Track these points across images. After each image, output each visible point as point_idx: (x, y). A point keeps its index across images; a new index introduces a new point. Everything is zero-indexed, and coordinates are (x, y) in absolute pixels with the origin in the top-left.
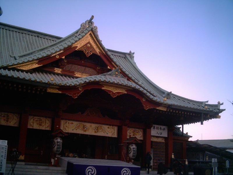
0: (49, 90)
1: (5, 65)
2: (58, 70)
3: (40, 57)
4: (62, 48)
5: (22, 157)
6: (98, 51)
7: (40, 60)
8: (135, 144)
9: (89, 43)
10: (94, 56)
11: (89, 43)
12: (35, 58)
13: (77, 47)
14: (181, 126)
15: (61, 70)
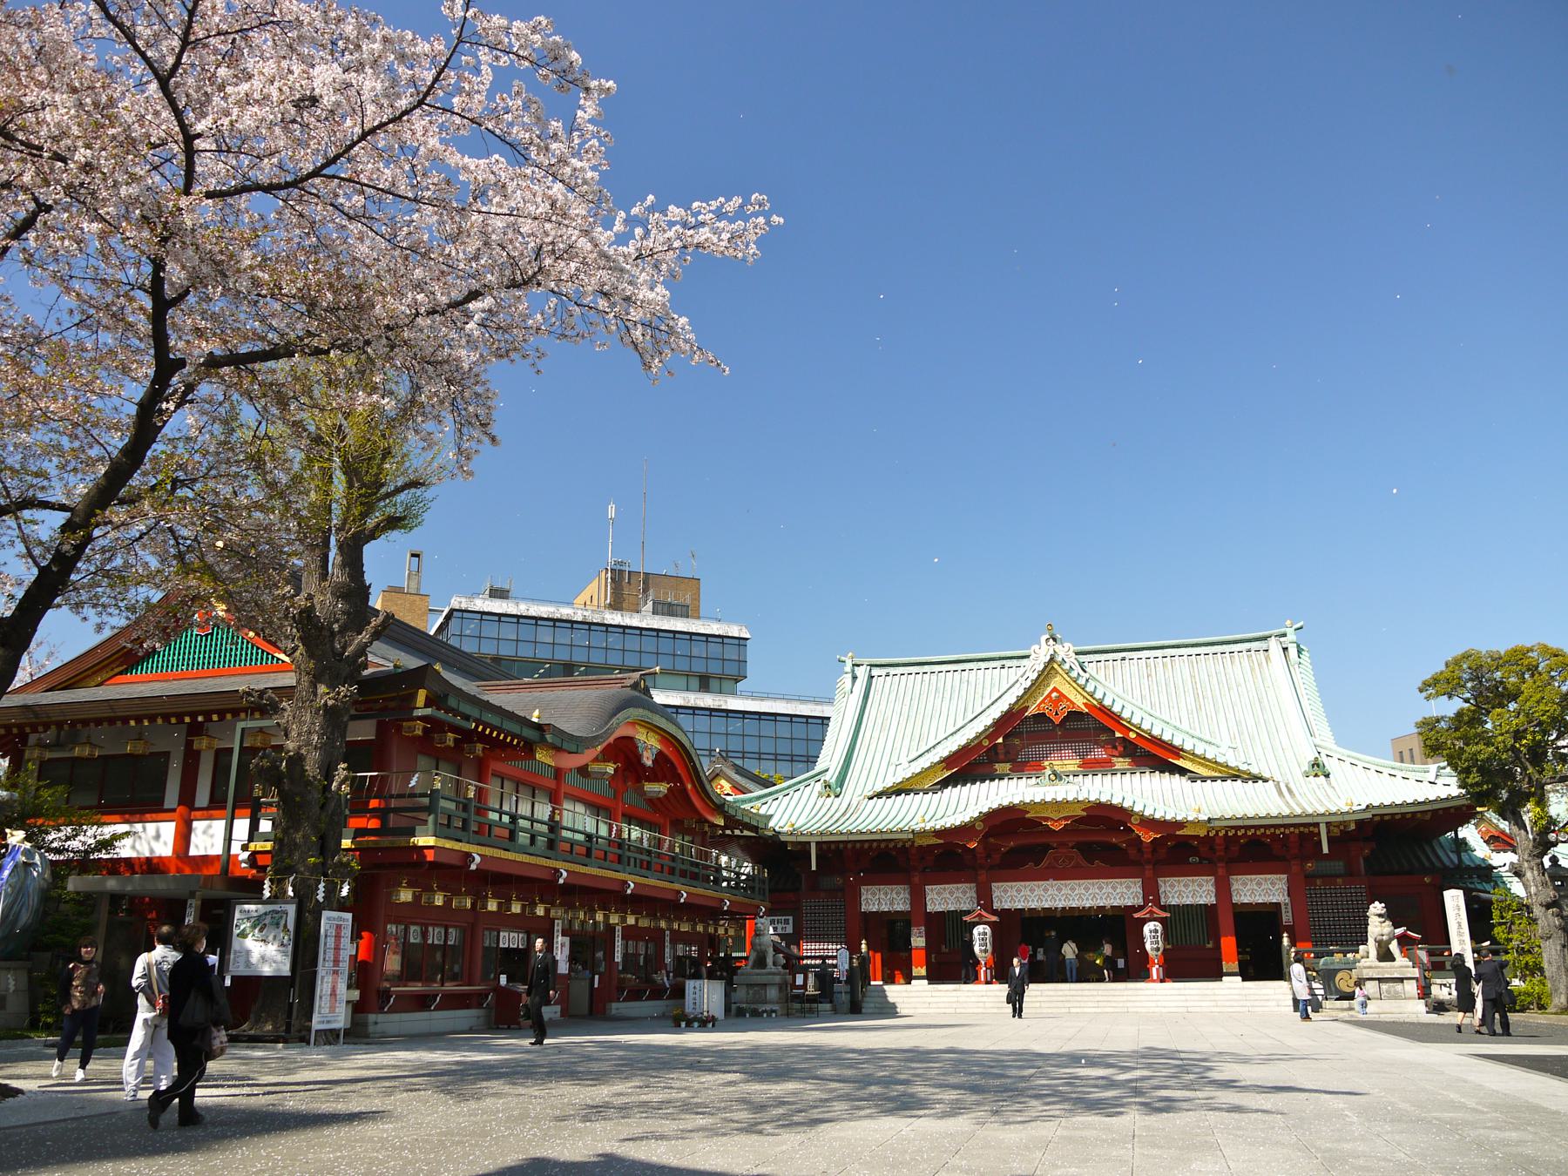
0: (919, 842)
1: (879, 788)
2: (1001, 768)
3: (946, 754)
4: (989, 722)
5: (923, 971)
6: (1079, 702)
7: (948, 761)
8: (1161, 920)
9: (1055, 689)
10: (1075, 715)
11: (1055, 689)
12: (937, 759)
13: (1027, 708)
14: (1451, 834)
15: (1008, 766)
